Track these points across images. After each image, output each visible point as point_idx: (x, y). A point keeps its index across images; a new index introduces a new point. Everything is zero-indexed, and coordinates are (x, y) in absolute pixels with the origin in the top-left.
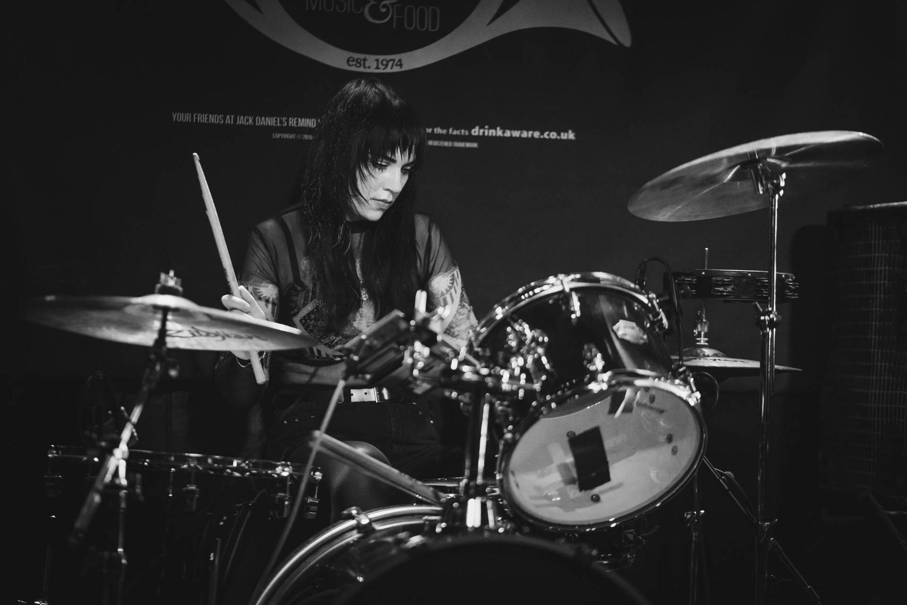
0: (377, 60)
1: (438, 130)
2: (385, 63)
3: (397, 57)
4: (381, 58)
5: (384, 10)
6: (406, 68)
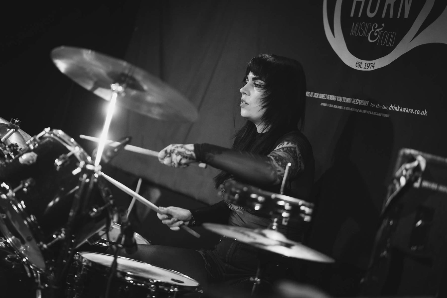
0: (366, 63)
1: (378, 106)
2: (368, 65)
3: (373, 62)
4: (367, 62)
5: (376, 34)
6: (375, 68)
